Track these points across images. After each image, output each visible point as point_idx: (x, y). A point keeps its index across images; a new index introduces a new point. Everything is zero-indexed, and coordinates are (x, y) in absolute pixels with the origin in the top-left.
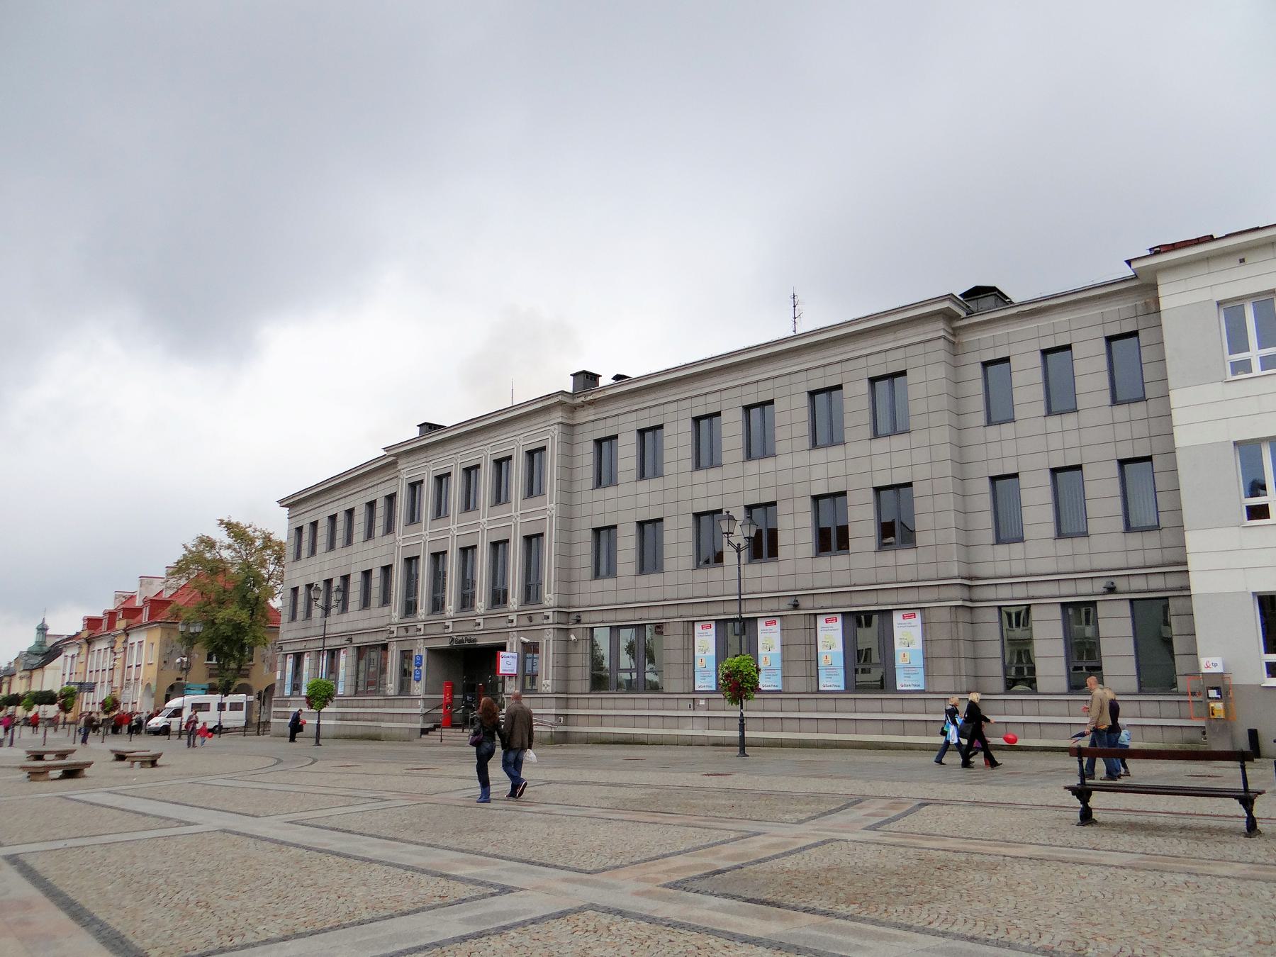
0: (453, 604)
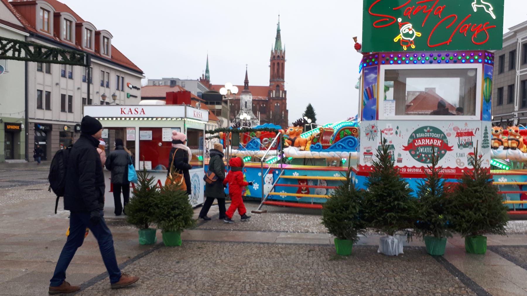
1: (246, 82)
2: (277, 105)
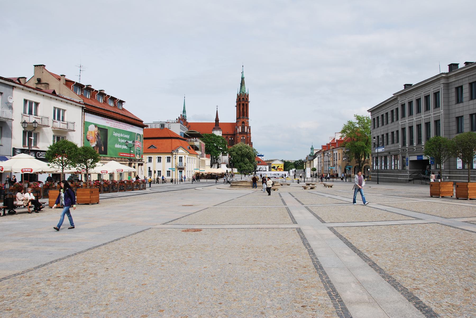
0: (415, 142)
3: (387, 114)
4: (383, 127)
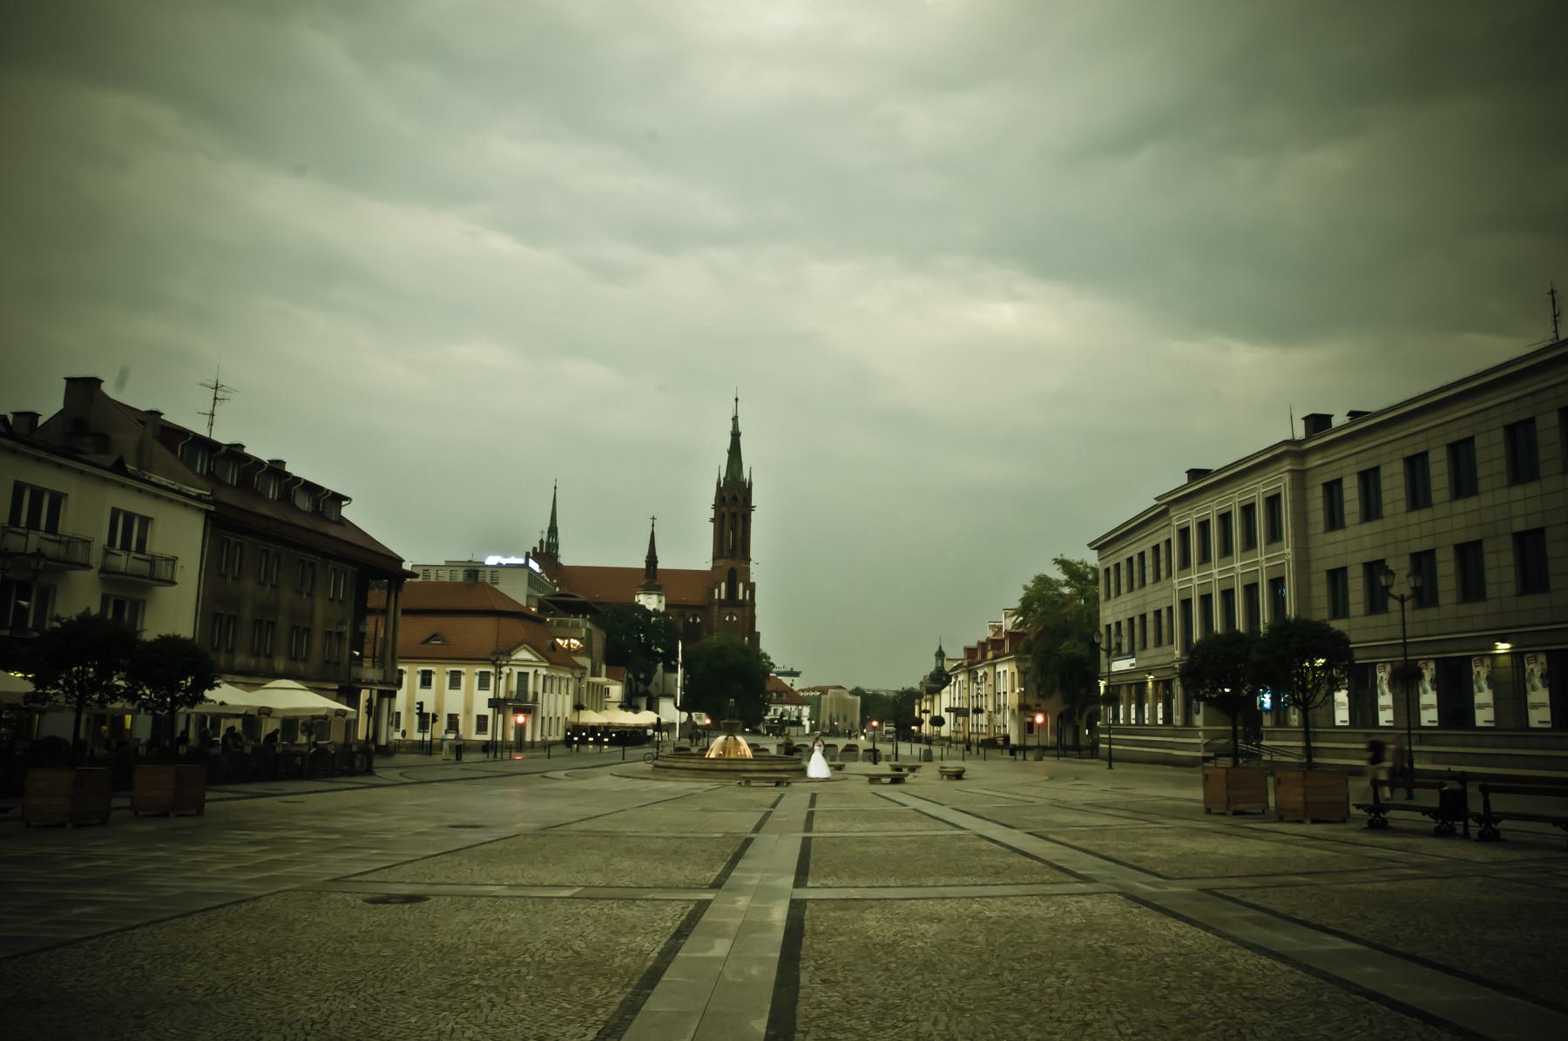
1: (652, 559)
2: (731, 618)
3: (1142, 555)
4: (1131, 596)
